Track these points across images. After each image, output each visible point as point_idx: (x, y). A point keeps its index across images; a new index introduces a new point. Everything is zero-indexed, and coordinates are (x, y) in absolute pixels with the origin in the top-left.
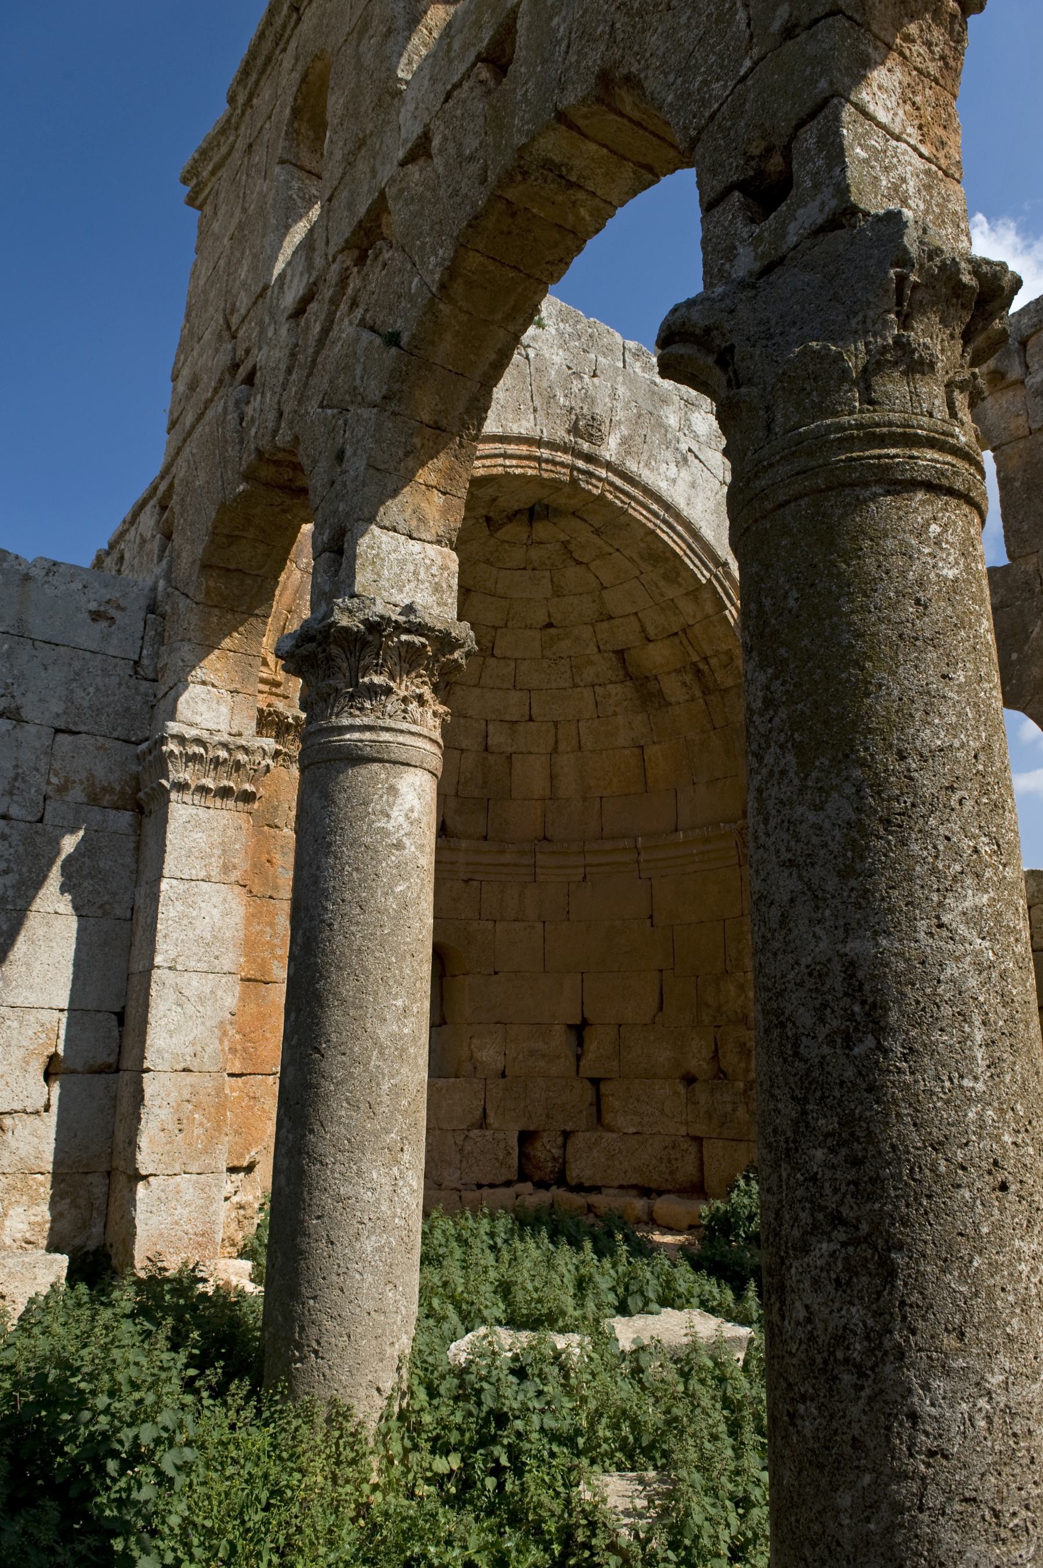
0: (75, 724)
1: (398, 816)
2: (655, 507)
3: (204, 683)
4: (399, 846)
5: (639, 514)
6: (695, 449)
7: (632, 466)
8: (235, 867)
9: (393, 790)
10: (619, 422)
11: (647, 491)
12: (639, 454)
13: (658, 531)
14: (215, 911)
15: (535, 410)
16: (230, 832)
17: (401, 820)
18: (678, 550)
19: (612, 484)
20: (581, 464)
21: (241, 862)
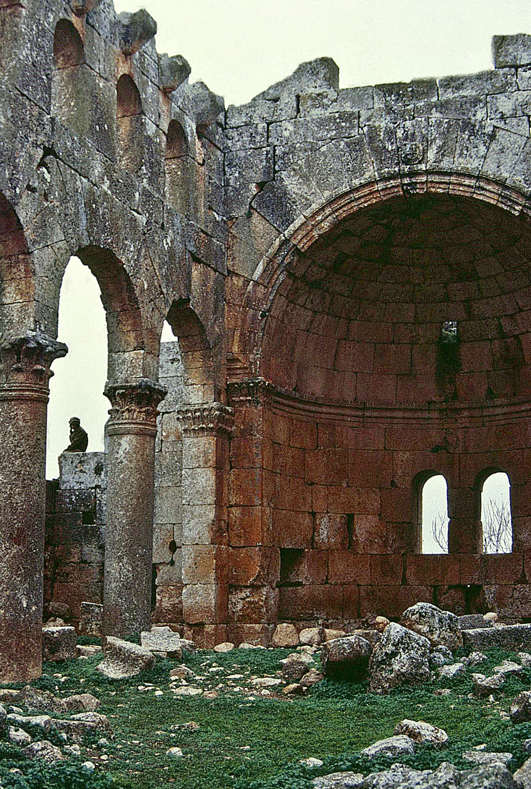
0: (169, 409)
1: (121, 452)
2: (467, 182)
3: (192, 385)
4: (122, 462)
5: (459, 191)
6: (501, 124)
7: (445, 164)
8: (210, 460)
9: (120, 444)
10: (435, 139)
11: (458, 174)
12: (453, 152)
13: (475, 196)
14: (203, 480)
15: (373, 163)
16: (207, 445)
17: (122, 453)
18: (492, 202)
19: (432, 182)
20: (406, 181)
21: (212, 457)
